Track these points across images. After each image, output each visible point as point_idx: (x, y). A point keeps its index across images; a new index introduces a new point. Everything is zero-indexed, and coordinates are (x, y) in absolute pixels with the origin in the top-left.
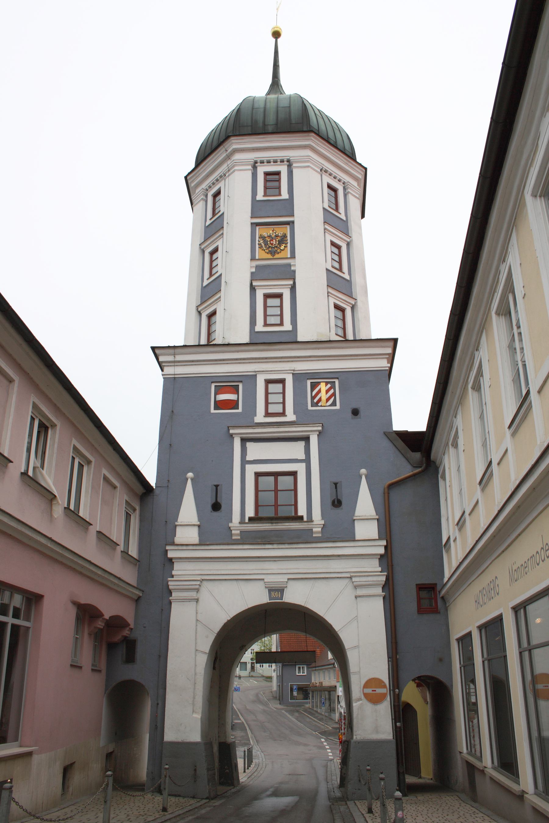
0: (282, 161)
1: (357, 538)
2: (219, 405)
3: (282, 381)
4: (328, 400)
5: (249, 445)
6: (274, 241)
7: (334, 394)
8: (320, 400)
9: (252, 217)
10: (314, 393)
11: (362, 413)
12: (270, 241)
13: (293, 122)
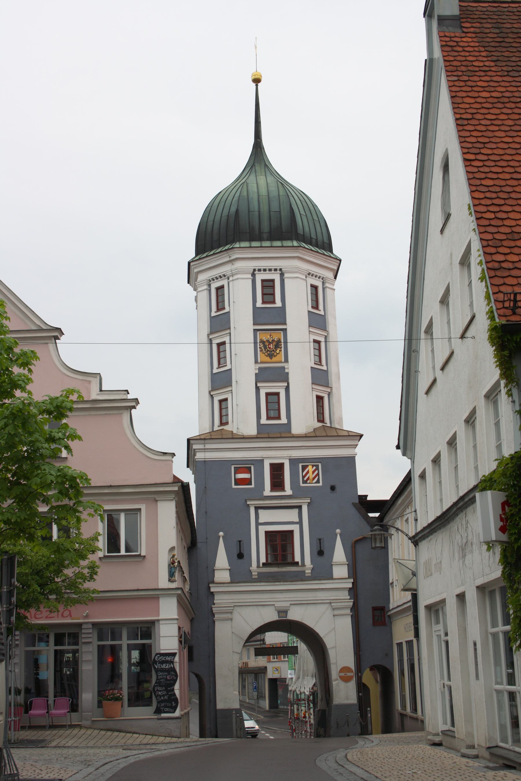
0: (276, 270)
1: (335, 576)
2: (238, 482)
4: (314, 479)
5: (260, 511)
7: (318, 474)
8: (308, 478)
9: (254, 324)
10: (304, 473)
11: (337, 489)
12: (269, 345)
13: (284, 230)
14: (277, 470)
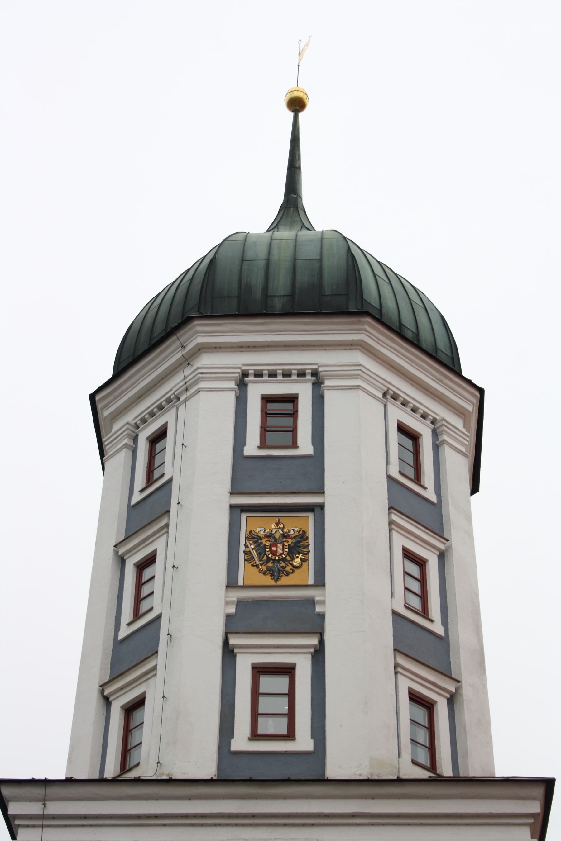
0: (301, 374)
6: (280, 546)
12: (271, 546)
13: (328, 291)
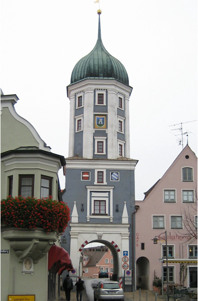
0: (104, 90)
2: (83, 178)
3: (103, 172)
9: (94, 112)
14: (100, 173)
